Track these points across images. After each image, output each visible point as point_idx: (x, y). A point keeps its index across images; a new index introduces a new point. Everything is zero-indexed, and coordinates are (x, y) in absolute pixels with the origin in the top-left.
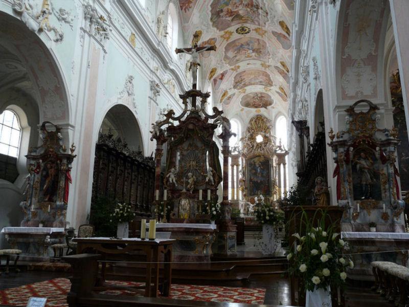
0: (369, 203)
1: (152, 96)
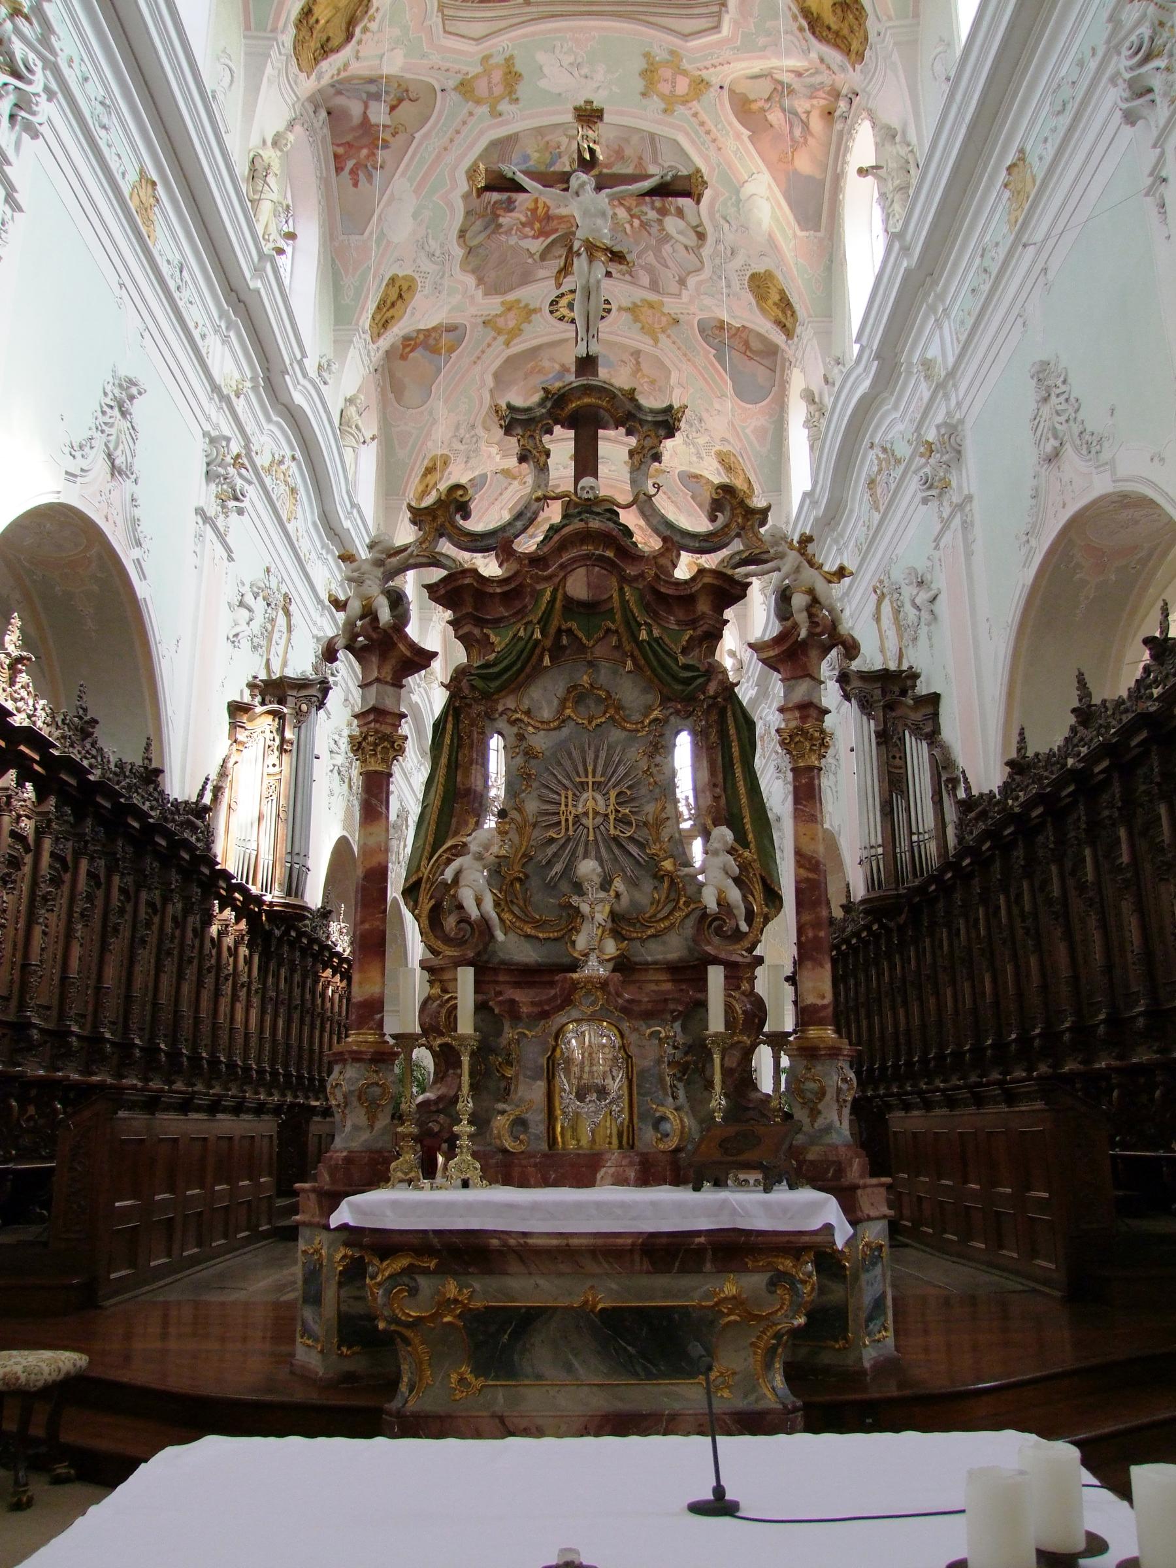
1: (212, 509)
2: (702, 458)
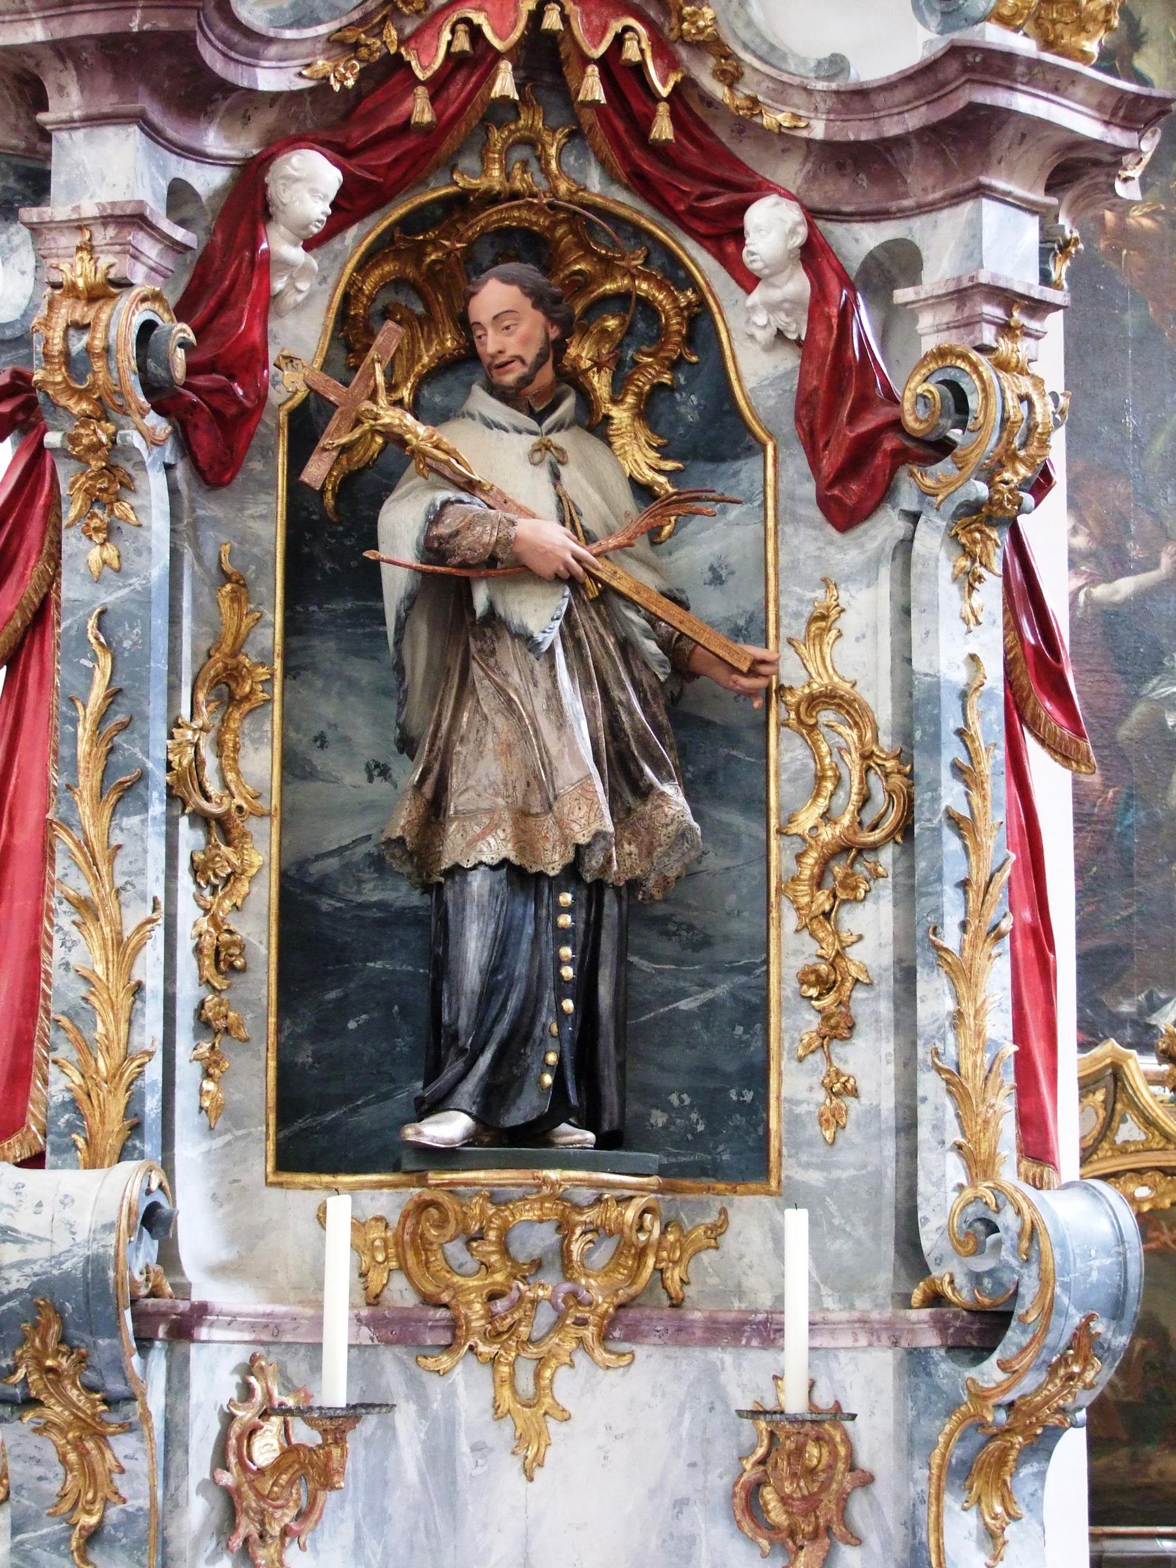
0: (538, 1239)
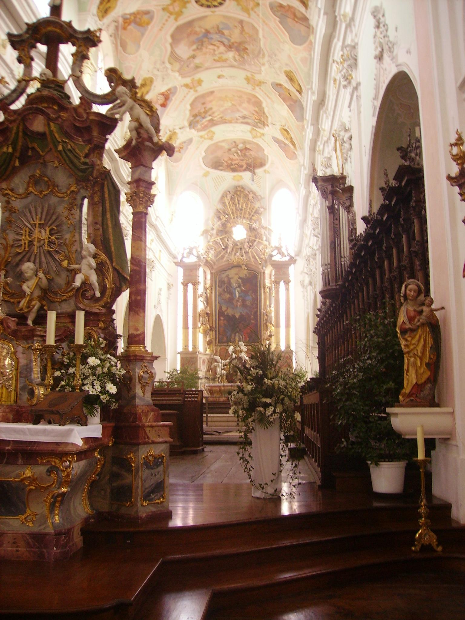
2: (279, 75)
